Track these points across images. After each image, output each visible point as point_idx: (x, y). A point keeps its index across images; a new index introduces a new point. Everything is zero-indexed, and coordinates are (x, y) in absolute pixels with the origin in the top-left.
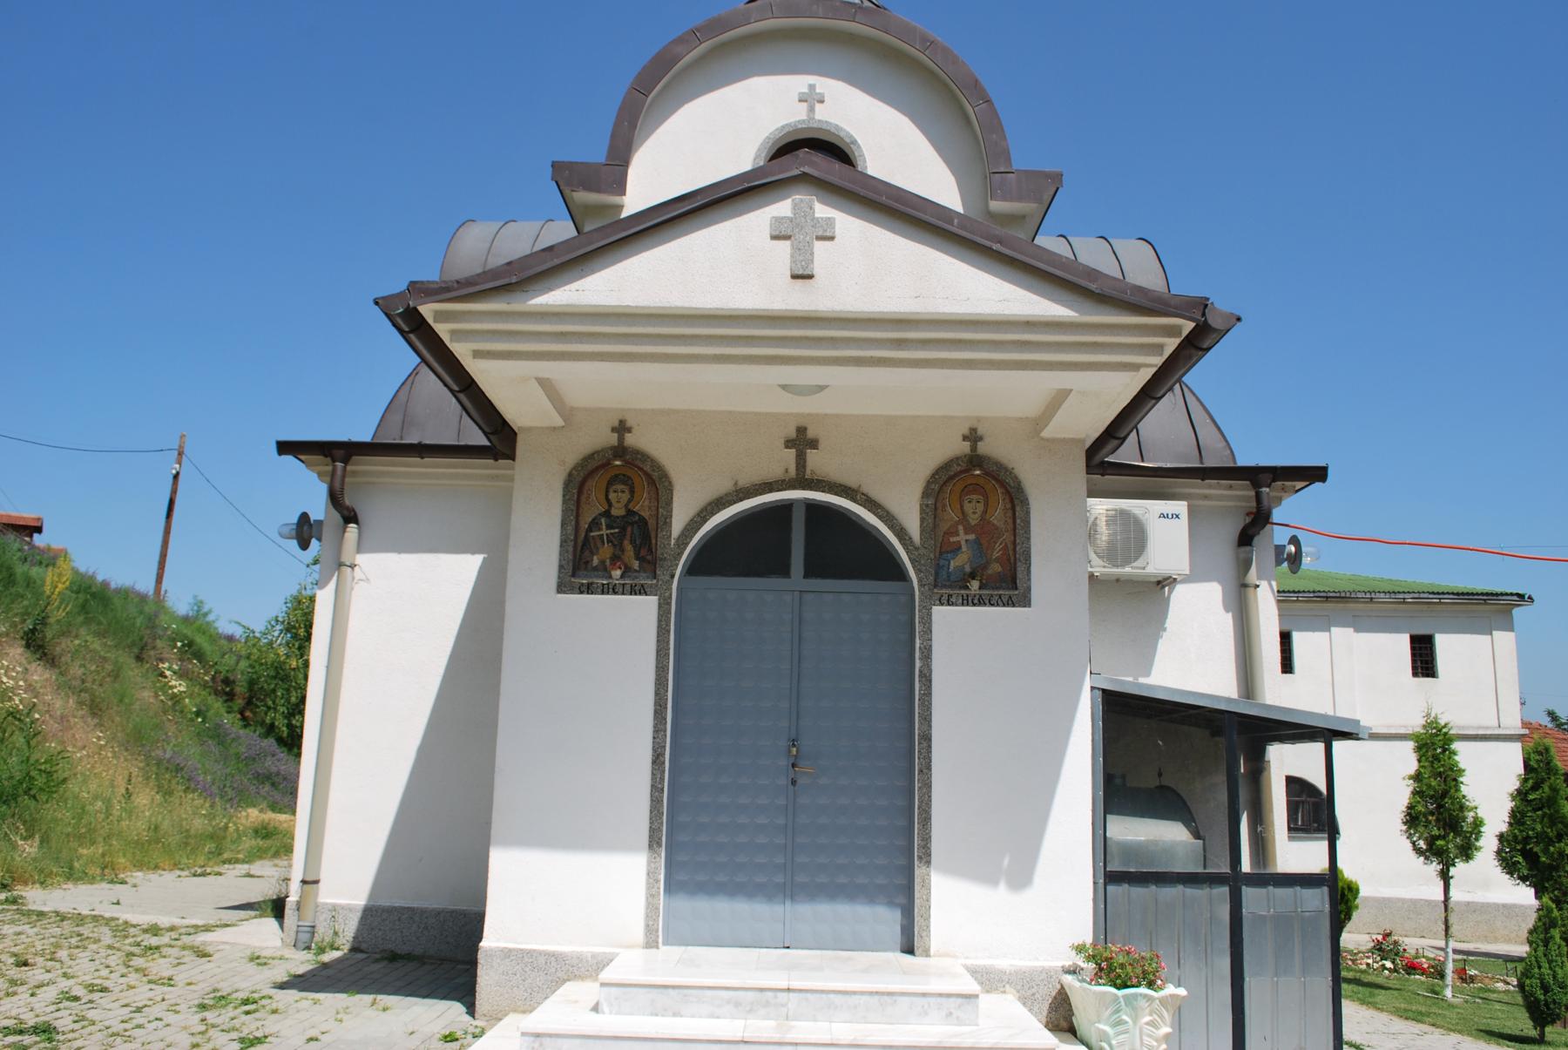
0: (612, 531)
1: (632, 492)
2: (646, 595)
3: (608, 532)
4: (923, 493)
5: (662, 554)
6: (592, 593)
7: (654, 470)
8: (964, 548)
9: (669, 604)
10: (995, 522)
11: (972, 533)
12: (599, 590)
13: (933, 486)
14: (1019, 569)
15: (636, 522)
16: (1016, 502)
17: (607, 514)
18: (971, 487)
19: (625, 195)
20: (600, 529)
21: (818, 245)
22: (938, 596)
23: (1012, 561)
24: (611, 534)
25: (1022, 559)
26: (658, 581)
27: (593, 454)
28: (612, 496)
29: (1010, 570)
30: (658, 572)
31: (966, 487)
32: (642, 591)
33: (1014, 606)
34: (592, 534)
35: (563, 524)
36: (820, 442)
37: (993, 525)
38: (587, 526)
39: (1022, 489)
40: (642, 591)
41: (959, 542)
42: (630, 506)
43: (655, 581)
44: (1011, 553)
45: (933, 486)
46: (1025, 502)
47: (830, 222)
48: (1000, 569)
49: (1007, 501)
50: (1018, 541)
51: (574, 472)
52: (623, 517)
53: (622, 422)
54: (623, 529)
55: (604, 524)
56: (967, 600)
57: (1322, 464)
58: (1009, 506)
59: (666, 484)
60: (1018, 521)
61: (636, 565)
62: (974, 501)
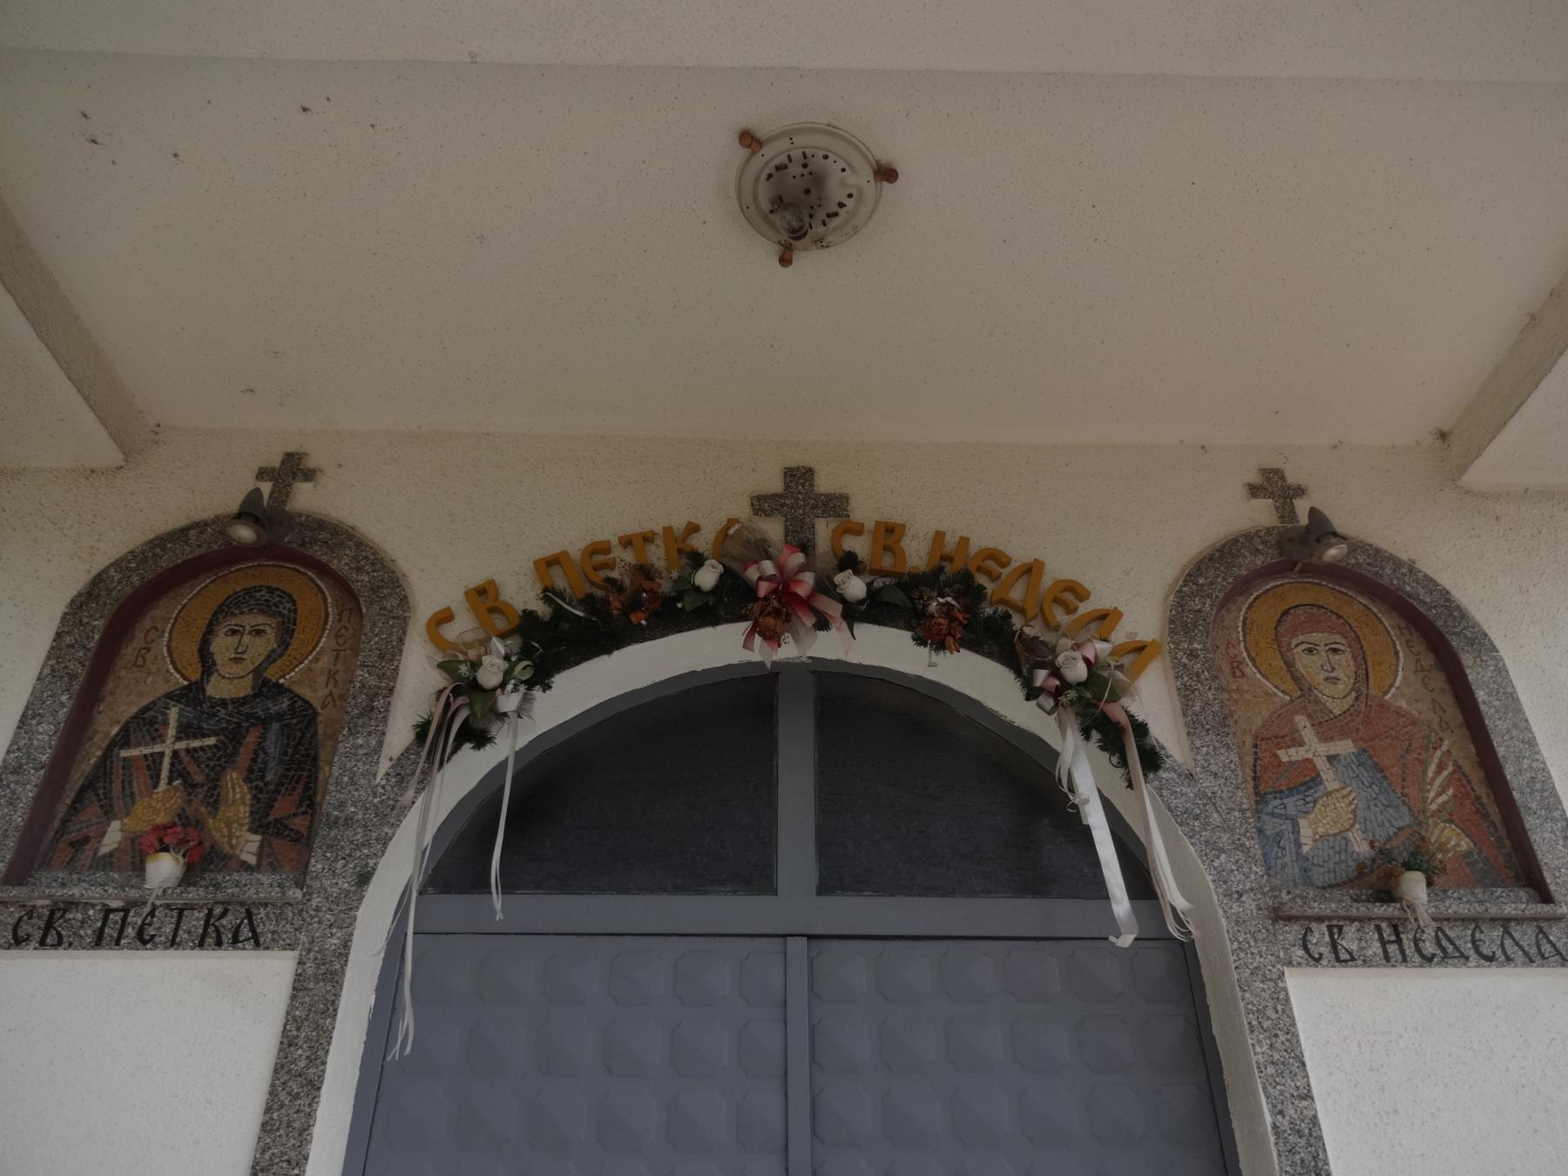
0: (196, 744)
1: (286, 632)
2: (257, 945)
3: (181, 745)
4: (1171, 622)
5: (341, 805)
6: (58, 944)
7: (359, 569)
8: (1330, 780)
9: (334, 979)
10: (1403, 704)
12: (88, 933)
13: (1196, 604)
15: (279, 717)
16: (1455, 642)
17: (192, 695)
18: (1300, 611)
20: (158, 737)
23: (1497, 818)
25: (1534, 806)
26: (308, 896)
27: (185, 530)
28: (222, 646)
30: (316, 866)
31: (1286, 613)
32: (245, 932)
34: (124, 754)
36: (853, 502)
37: (1399, 713)
38: (115, 730)
39: (1458, 607)
40: (245, 932)
42: (272, 673)
44: (1482, 791)
45: (1196, 604)
46: (1481, 642)
49: (1419, 646)
50: (1501, 751)
51: (112, 573)
52: (244, 701)
54: (234, 737)
55: (173, 723)
56: (1399, 941)
58: (1428, 660)
59: (391, 603)
60: (1481, 695)
61: (249, 846)
62: (1322, 649)
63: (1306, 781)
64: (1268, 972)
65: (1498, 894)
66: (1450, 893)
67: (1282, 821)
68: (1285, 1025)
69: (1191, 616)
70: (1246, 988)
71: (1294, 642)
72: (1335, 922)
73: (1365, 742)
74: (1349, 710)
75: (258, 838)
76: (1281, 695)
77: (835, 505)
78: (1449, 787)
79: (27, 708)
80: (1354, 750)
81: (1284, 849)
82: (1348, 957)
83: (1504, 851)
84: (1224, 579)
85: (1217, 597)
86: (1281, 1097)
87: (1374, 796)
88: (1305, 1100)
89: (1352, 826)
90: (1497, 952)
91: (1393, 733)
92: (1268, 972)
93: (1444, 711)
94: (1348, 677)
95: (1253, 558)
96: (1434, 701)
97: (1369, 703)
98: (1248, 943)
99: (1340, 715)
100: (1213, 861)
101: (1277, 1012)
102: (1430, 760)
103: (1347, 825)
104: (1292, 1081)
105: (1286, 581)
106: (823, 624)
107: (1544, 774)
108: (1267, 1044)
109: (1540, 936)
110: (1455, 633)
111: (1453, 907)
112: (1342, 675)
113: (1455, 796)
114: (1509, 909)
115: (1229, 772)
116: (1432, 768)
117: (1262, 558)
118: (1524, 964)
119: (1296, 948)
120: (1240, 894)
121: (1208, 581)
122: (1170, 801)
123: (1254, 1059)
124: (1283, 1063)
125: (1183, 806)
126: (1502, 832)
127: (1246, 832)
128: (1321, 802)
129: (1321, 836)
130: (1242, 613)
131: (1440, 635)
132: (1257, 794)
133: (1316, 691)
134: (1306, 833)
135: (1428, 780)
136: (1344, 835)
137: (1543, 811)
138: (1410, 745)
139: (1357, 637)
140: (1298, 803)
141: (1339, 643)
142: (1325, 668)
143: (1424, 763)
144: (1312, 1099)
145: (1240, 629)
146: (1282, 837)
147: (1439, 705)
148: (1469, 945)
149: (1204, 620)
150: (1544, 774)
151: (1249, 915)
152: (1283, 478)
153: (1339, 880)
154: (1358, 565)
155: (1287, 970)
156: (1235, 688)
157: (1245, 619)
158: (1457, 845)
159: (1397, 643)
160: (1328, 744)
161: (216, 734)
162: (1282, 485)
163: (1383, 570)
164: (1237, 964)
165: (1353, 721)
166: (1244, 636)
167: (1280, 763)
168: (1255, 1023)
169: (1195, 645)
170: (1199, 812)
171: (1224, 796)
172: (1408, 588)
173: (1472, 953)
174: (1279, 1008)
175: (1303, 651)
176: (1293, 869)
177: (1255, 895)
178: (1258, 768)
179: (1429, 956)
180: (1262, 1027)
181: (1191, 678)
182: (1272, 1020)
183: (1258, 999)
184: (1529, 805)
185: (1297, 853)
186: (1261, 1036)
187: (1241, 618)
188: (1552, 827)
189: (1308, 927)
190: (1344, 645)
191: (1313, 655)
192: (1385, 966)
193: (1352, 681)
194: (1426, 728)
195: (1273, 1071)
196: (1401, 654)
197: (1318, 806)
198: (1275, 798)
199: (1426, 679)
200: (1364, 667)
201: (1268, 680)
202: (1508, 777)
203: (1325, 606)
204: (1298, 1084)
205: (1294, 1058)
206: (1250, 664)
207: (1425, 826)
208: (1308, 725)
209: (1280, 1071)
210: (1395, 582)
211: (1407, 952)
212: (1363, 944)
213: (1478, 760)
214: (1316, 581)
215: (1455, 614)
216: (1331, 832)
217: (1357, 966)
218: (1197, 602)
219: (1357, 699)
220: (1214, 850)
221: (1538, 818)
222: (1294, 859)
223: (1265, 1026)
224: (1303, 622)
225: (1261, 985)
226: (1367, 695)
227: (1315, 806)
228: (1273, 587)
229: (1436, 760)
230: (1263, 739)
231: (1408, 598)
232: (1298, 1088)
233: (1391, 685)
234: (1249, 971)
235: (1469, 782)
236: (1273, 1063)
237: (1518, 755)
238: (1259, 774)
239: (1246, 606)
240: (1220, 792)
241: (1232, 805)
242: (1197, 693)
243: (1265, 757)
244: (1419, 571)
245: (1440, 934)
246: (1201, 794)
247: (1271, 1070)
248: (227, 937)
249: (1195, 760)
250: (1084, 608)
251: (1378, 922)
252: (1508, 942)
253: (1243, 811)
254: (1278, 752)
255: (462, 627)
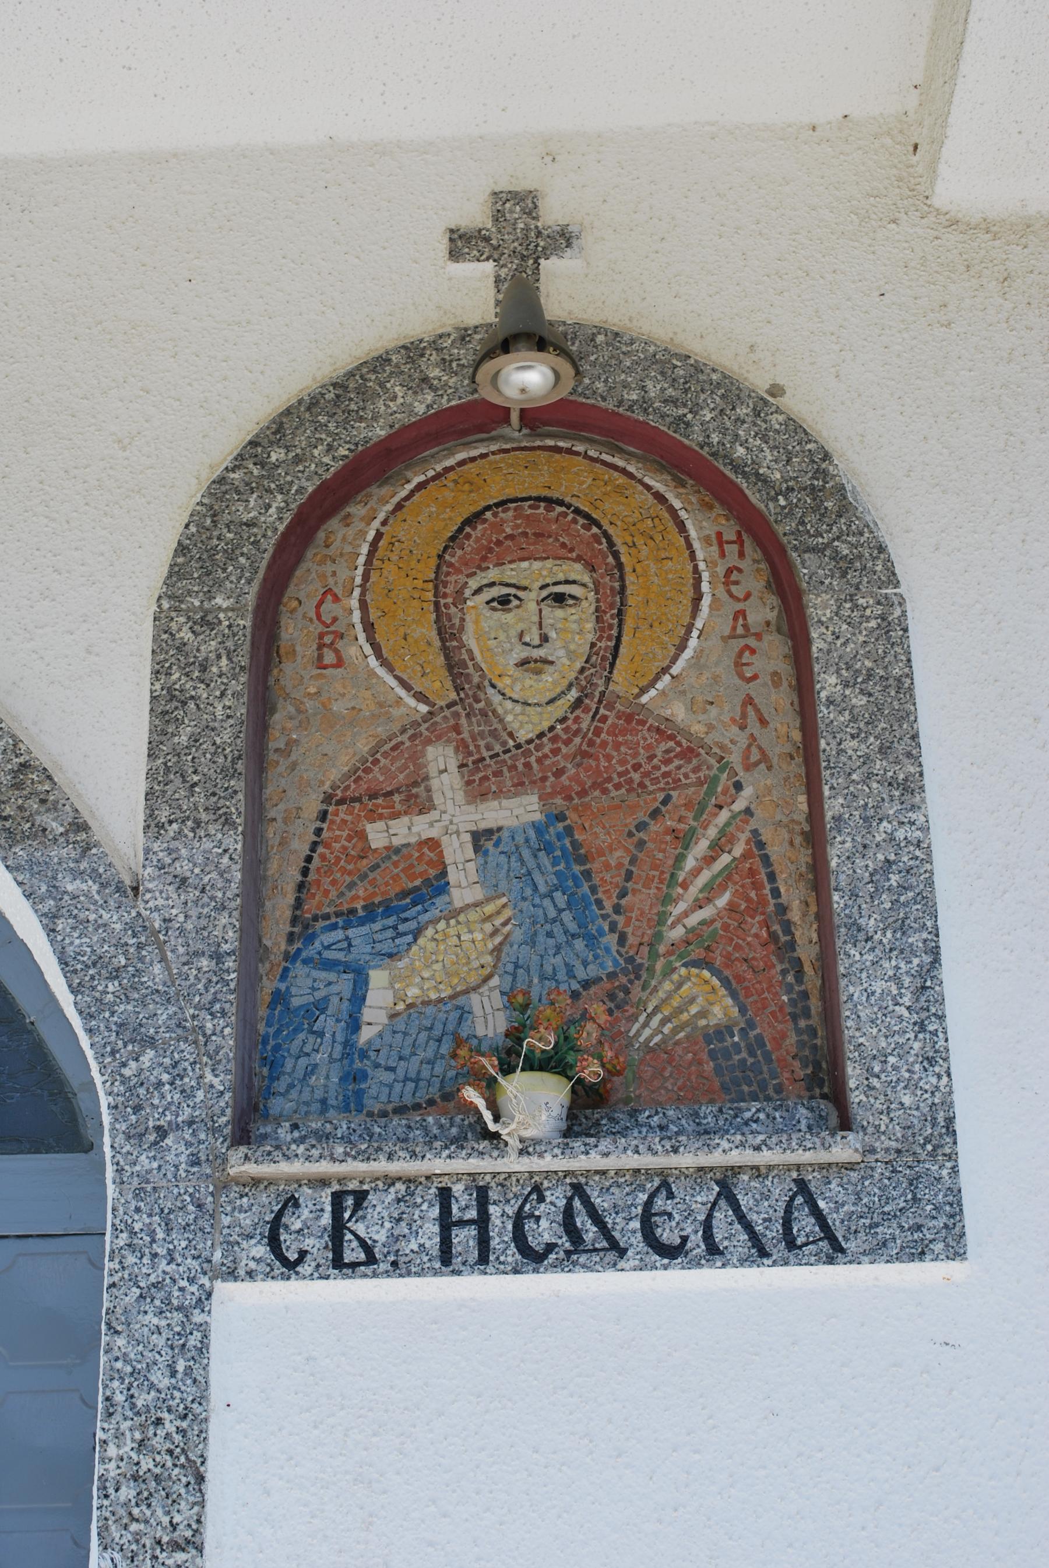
4: (182, 549)
10: (678, 711)
11: (520, 786)
14: (851, 991)
22: (266, 1203)
23: (807, 952)
25: (871, 924)
29: (800, 1009)
31: (475, 518)
37: (665, 731)
50: (833, 806)
56: (483, 1222)
60: (828, 684)
64: (176, 1294)
65: (747, 1115)
66: (642, 1118)
67: (332, 976)
68: (182, 1400)
69: (230, 536)
70: (119, 1328)
71: (473, 584)
72: (352, 1186)
73: (569, 798)
74: (552, 728)
76: (412, 702)
78: (723, 888)
80: (537, 817)
81: (321, 1034)
82: (362, 1257)
83: (802, 1023)
84: (330, 448)
85: (301, 490)
86: (134, 1547)
87: (552, 913)
88: (183, 1550)
89: (487, 979)
90: (692, 1237)
91: (636, 777)
92: (176, 1294)
93: (763, 722)
94: (571, 655)
95: (409, 399)
96: (749, 701)
97: (602, 711)
98: (152, 1233)
99: (529, 742)
100: (124, 1065)
101: (173, 1374)
102: (700, 831)
103: (473, 979)
104: (168, 1513)
105: (494, 447)
107: (918, 853)
108: (133, 1440)
109: (799, 1200)
110: (813, 550)
112: (562, 653)
113: (732, 908)
115: (214, 875)
116: (701, 847)
117: (429, 397)
118: (743, 1262)
119: (253, 1241)
120: (162, 1132)
121: (291, 455)
122: (67, 941)
123: (98, 1470)
124: (157, 1478)
125: (93, 951)
126: (812, 979)
127: (215, 1000)
128: (430, 932)
129: (410, 1006)
130: (376, 524)
131: (782, 551)
132: (294, 920)
133: (490, 691)
135: (681, 876)
136: (461, 1001)
137: (889, 934)
138: (666, 801)
139: (620, 566)
140: (378, 937)
141: (574, 582)
142: (527, 639)
143: (685, 839)
144: (200, 1549)
145: (362, 560)
146: (323, 1011)
147: (758, 711)
148: (636, 1224)
149: (256, 543)
150: (918, 853)
151: (170, 1176)
152: (532, 212)
153: (422, 1096)
154: (645, 404)
155: (223, 1289)
156: (312, 690)
157: (379, 535)
158: (703, 1014)
159: (705, 576)
160: (482, 807)
162: (527, 229)
163: (696, 413)
164: (116, 1278)
165: (556, 752)
166: (366, 577)
167: (366, 851)
168: (119, 1398)
169: (219, 600)
170: (123, 962)
171: (189, 926)
172: (741, 451)
173: (637, 1241)
174: (181, 1366)
175: (488, 603)
176: (327, 1077)
177: (194, 1134)
178: (316, 862)
179: (540, 1249)
180: (133, 1406)
181: (187, 675)
182: (159, 1391)
183: (140, 1348)
184: (862, 922)
185: (346, 1044)
186: (125, 1425)
187: (371, 535)
188: (897, 968)
189: (293, 1196)
190: (584, 585)
191: (510, 610)
192: (436, 1273)
193: (578, 665)
194: (712, 761)
195: (133, 1493)
196: (706, 602)
197: (421, 941)
198: (334, 927)
199: (747, 653)
200: (614, 632)
201: (391, 669)
202: (833, 864)
203: (567, 499)
204: (177, 1519)
205: (183, 1466)
206: (362, 637)
207: (644, 975)
208: (453, 765)
209: (146, 1494)
210: (715, 438)
211: (495, 1243)
212: (403, 1226)
213: (807, 828)
214: (561, 444)
215: (829, 504)
216: (433, 996)
217: (375, 1275)
218: (252, 504)
219: (578, 703)
220: (133, 1041)
221: (873, 949)
222: (336, 1055)
223: (139, 1403)
224: (511, 537)
225: (155, 1321)
226: (602, 694)
227: (415, 940)
228: (462, 463)
229: (712, 832)
230: (341, 802)
231: (732, 476)
232: (174, 1527)
233: (665, 670)
234: (138, 1291)
235: (772, 877)
236: (135, 1478)
237: (871, 812)
238: (312, 876)
239: (389, 507)
240: (181, 918)
241: (200, 946)
242: (192, 705)
243: (337, 839)
244: (778, 411)
245: (577, 1203)
246: (138, 926)
247: (128, 1492)
249: (147, 851)
251: (446, 1182)
252: (723, 1216)
253: (218, 957)
254: (369, 827)
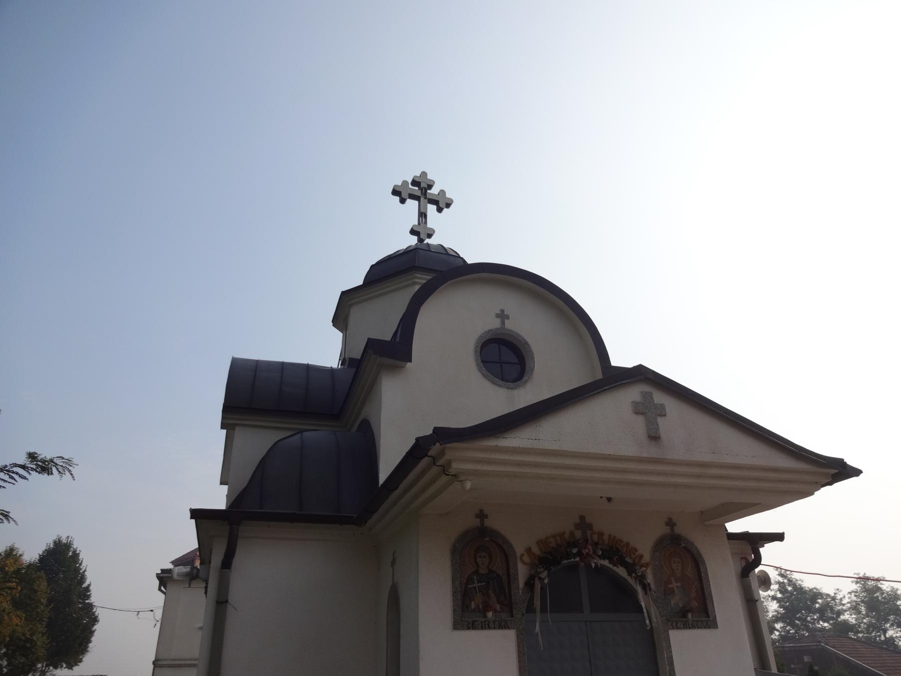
0: (481, 584)
3: (479, 584)
6: (475, 629)
12: (479, 626)
17: (476, 572)
19: (411, 361)
20: (474, 583)
21: (660, 420)
24: (481, 586)
26: (515, 619)
28: (479, 560)
30: (514, 612)
32: (506, 626)
33: (710, 628)
34: (469, 586)
35: (453, 581)
40: (506, 626)
41: (673, 588)
43: (514, 619)
46: (704, 562)
47: (662, 406)
48: (697, 605)
50: (705, 587)
53: (481, 511)
57: (781, 532)
60: (703, 575)
61: (498, 607)
63: (672, 592)
75: (499, 605)
77: (590, 526)
79: (452, 578)
106: (593, 558)
111: (695, 619)
114: (703, 619)
134: (672, 603)
161: (485, 582)
247: (666, 648)
248: (503, 627)
250: (637, 553)
255: (526, 559)
